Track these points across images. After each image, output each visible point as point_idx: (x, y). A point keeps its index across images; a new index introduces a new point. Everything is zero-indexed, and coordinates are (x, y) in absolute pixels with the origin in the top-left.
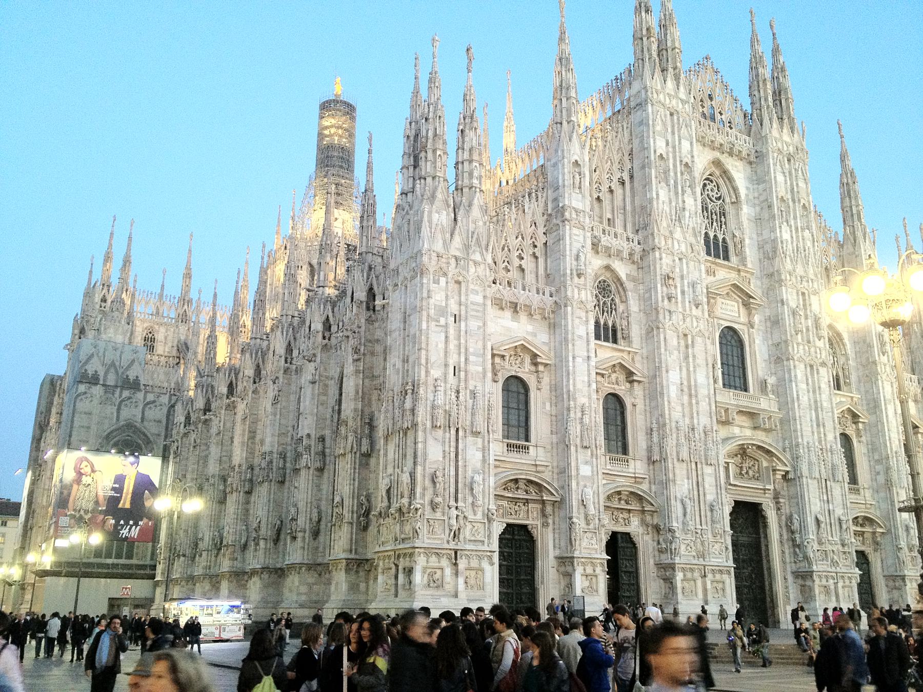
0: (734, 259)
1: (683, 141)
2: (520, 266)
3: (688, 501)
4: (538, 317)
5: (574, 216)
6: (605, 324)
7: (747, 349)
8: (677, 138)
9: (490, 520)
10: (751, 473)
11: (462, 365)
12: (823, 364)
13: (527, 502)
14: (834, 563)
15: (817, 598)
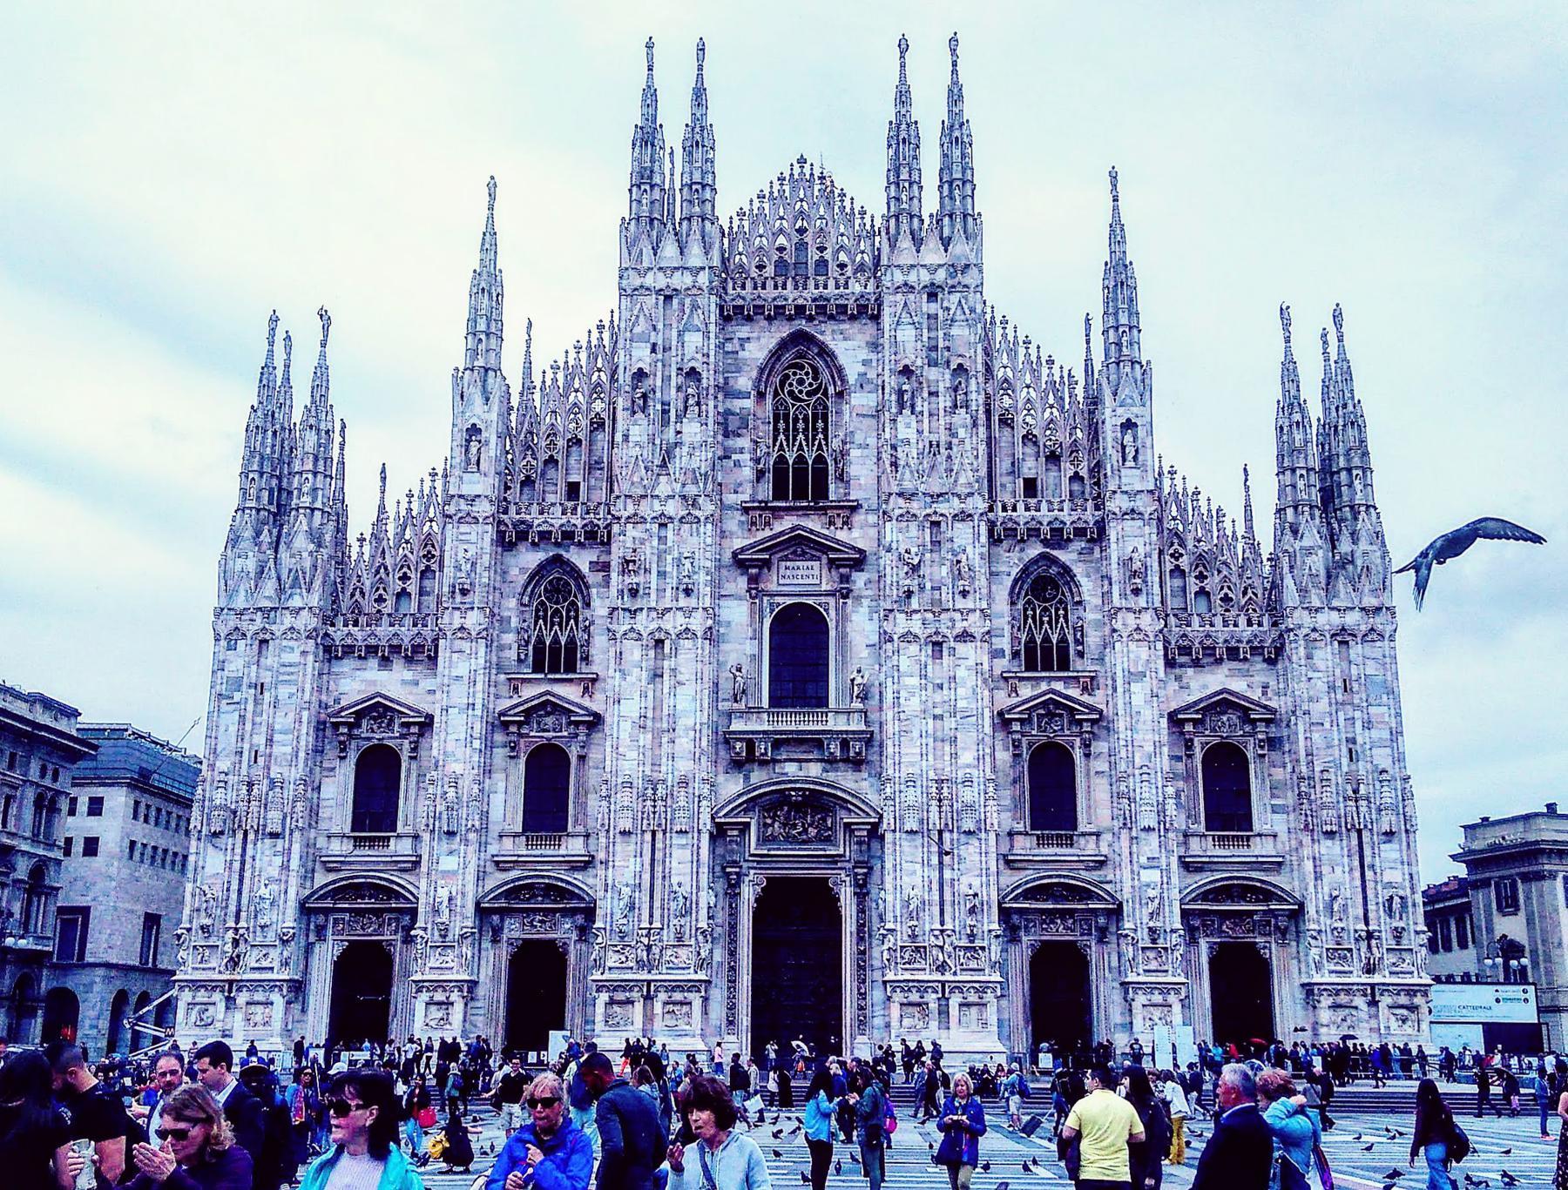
0: (832, 487)
1: (687, 337)
2: (404, 589)
3: (626, 891)
4: (420, 657)
5: (463, 506)
6: (556, 640)
7: (832, 633)
8: (674, 333)
9: (285, 943)
10: (812, 832)
11: (262, 748)
12: (965, 636)
13: (378, 913)
14: (942, 968)
15: (895, 1023)
